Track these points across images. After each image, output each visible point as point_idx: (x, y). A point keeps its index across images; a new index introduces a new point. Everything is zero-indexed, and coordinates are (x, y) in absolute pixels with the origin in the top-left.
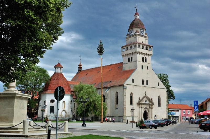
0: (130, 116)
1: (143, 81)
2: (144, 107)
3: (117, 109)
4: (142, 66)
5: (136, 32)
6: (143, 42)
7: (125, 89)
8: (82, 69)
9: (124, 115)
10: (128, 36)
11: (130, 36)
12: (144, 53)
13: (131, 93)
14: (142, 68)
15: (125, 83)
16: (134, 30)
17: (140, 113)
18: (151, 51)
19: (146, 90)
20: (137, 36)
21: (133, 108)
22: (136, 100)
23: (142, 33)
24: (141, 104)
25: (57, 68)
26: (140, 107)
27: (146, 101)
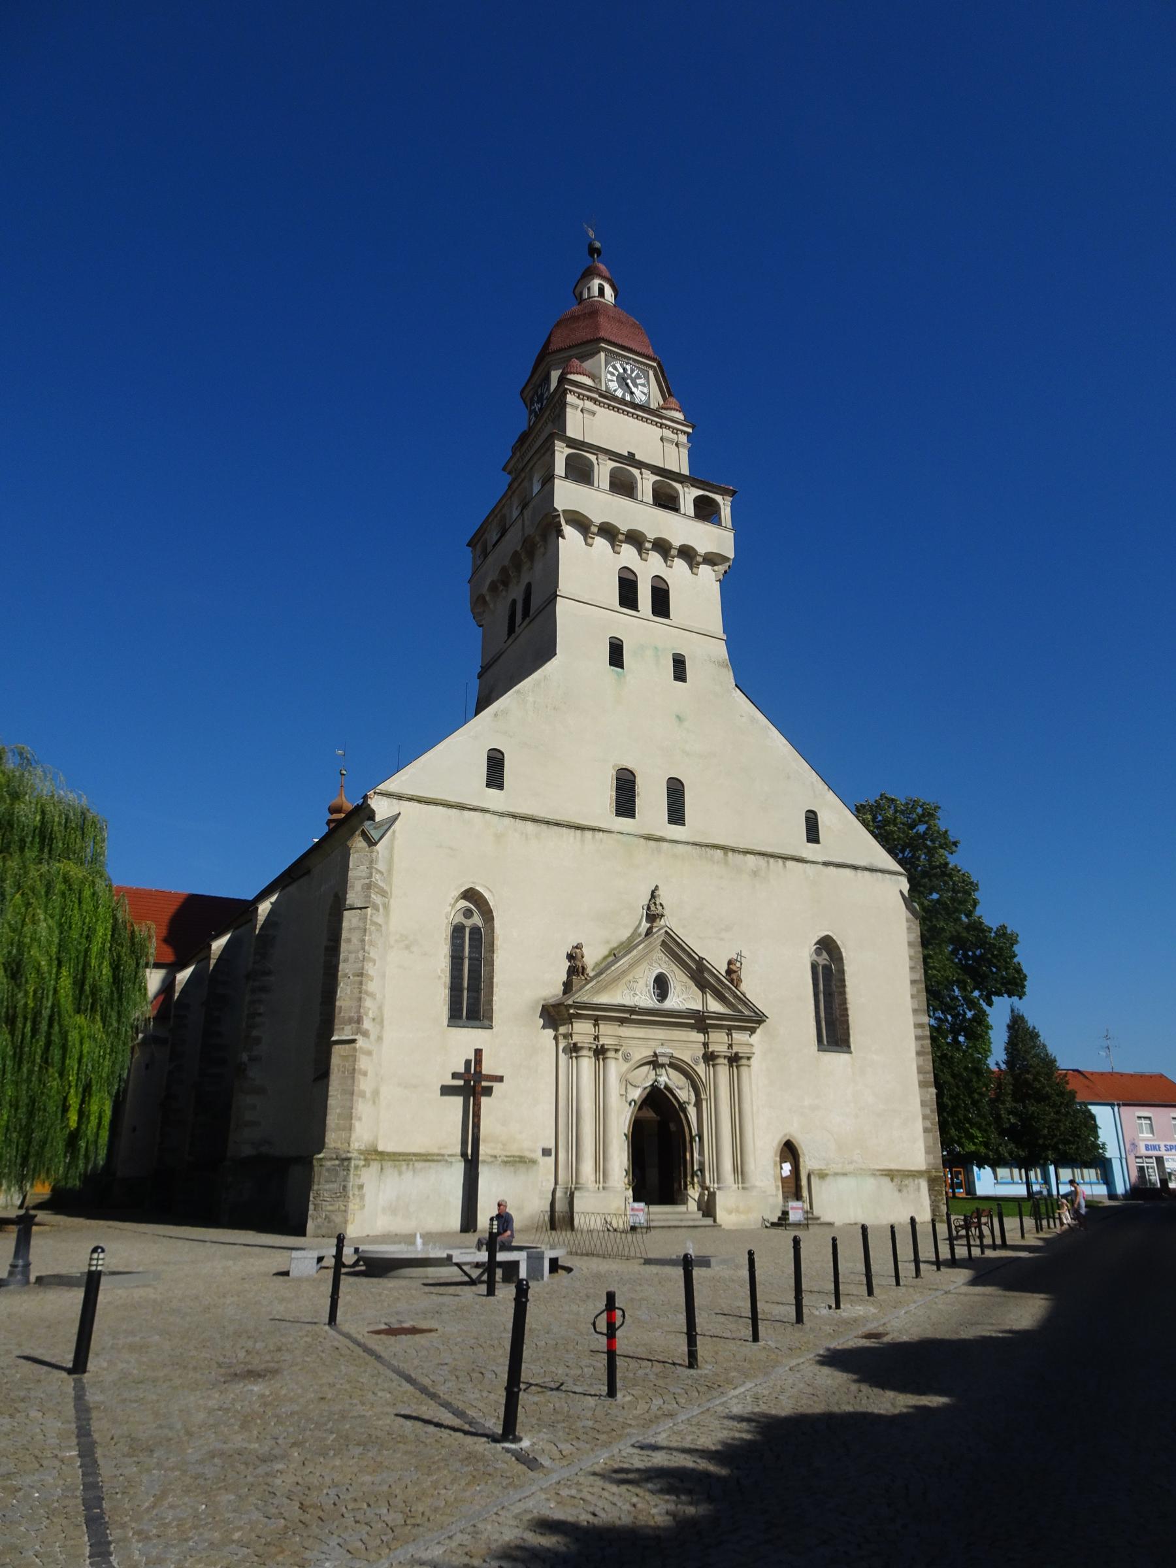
0: (426, 1158)
12: (635, 539)
21: (478, 1052)
22: (524, 974)
24: (599, 1015)
27: (661, 985)
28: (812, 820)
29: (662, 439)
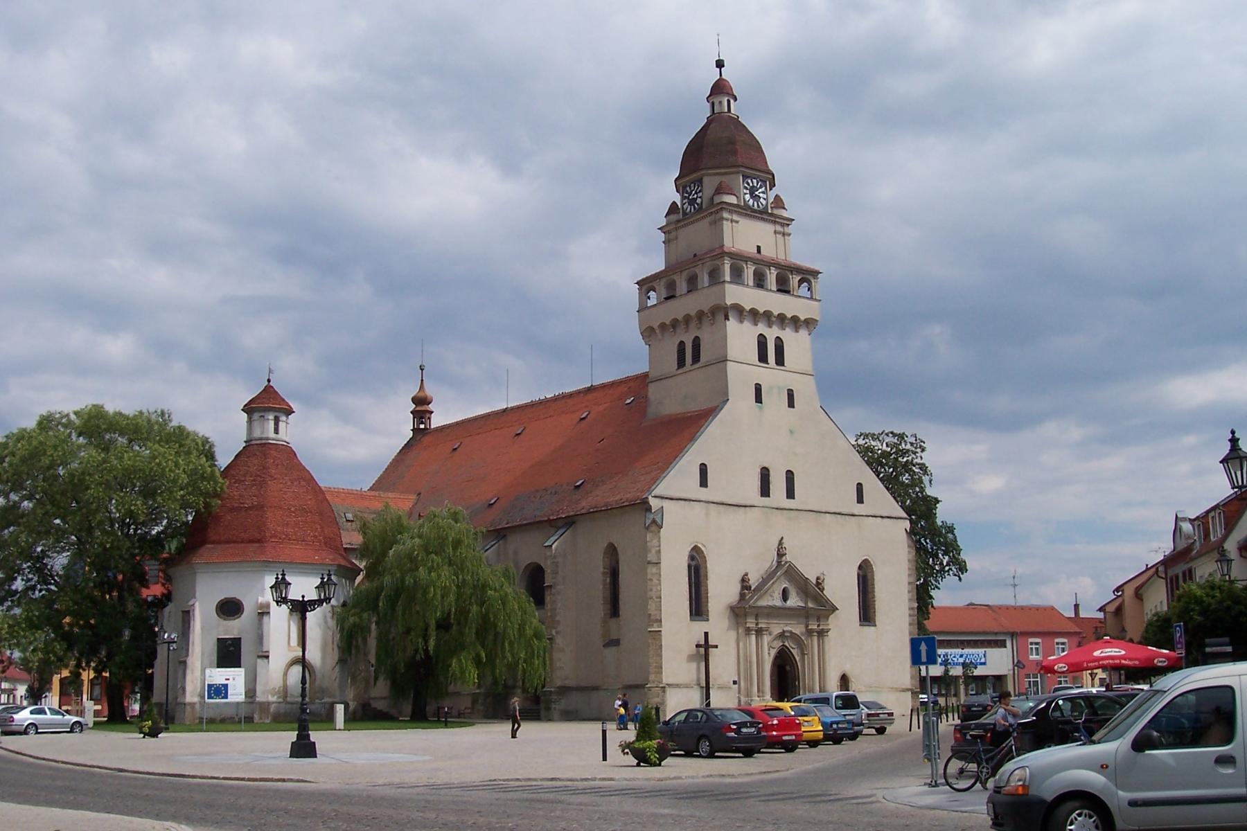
1: (765, 475)
2: (777, 630)
3: (615, 643)
4: (758, 389)
5: (719, 190)
6: (759, 248)
7: (654, 528)
8: (437, 421)
9: (652, 677)
10: (673, 217)
11: (685, 214)
12: (767, 315)
13: (696, 549)
14: (759, 399)
15: (657, 491)
16: (706, 180)
17: (748, 662)
18: (811, 298)
19: (781, 527)
20: (725, 215)
21: (706, 634)
22: (722, 591)
23: (752, 194)
24: (759, 613)
25: (256, 416)
26: (748, 630)
27: (785, 595)
28: (860, 487)
29: (775, 232)
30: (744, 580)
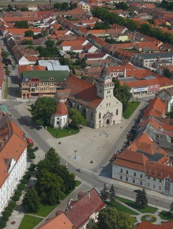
22: (102, 115)
30: (104, 114)
